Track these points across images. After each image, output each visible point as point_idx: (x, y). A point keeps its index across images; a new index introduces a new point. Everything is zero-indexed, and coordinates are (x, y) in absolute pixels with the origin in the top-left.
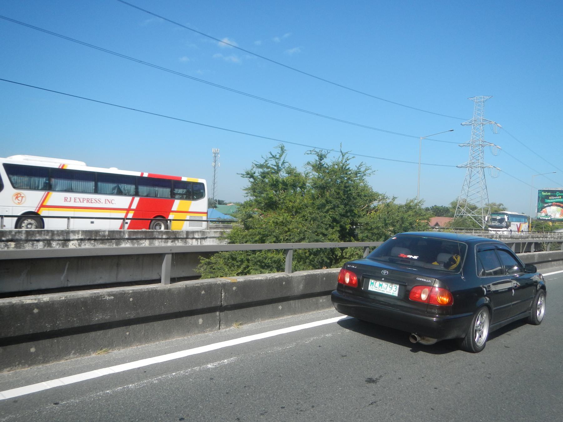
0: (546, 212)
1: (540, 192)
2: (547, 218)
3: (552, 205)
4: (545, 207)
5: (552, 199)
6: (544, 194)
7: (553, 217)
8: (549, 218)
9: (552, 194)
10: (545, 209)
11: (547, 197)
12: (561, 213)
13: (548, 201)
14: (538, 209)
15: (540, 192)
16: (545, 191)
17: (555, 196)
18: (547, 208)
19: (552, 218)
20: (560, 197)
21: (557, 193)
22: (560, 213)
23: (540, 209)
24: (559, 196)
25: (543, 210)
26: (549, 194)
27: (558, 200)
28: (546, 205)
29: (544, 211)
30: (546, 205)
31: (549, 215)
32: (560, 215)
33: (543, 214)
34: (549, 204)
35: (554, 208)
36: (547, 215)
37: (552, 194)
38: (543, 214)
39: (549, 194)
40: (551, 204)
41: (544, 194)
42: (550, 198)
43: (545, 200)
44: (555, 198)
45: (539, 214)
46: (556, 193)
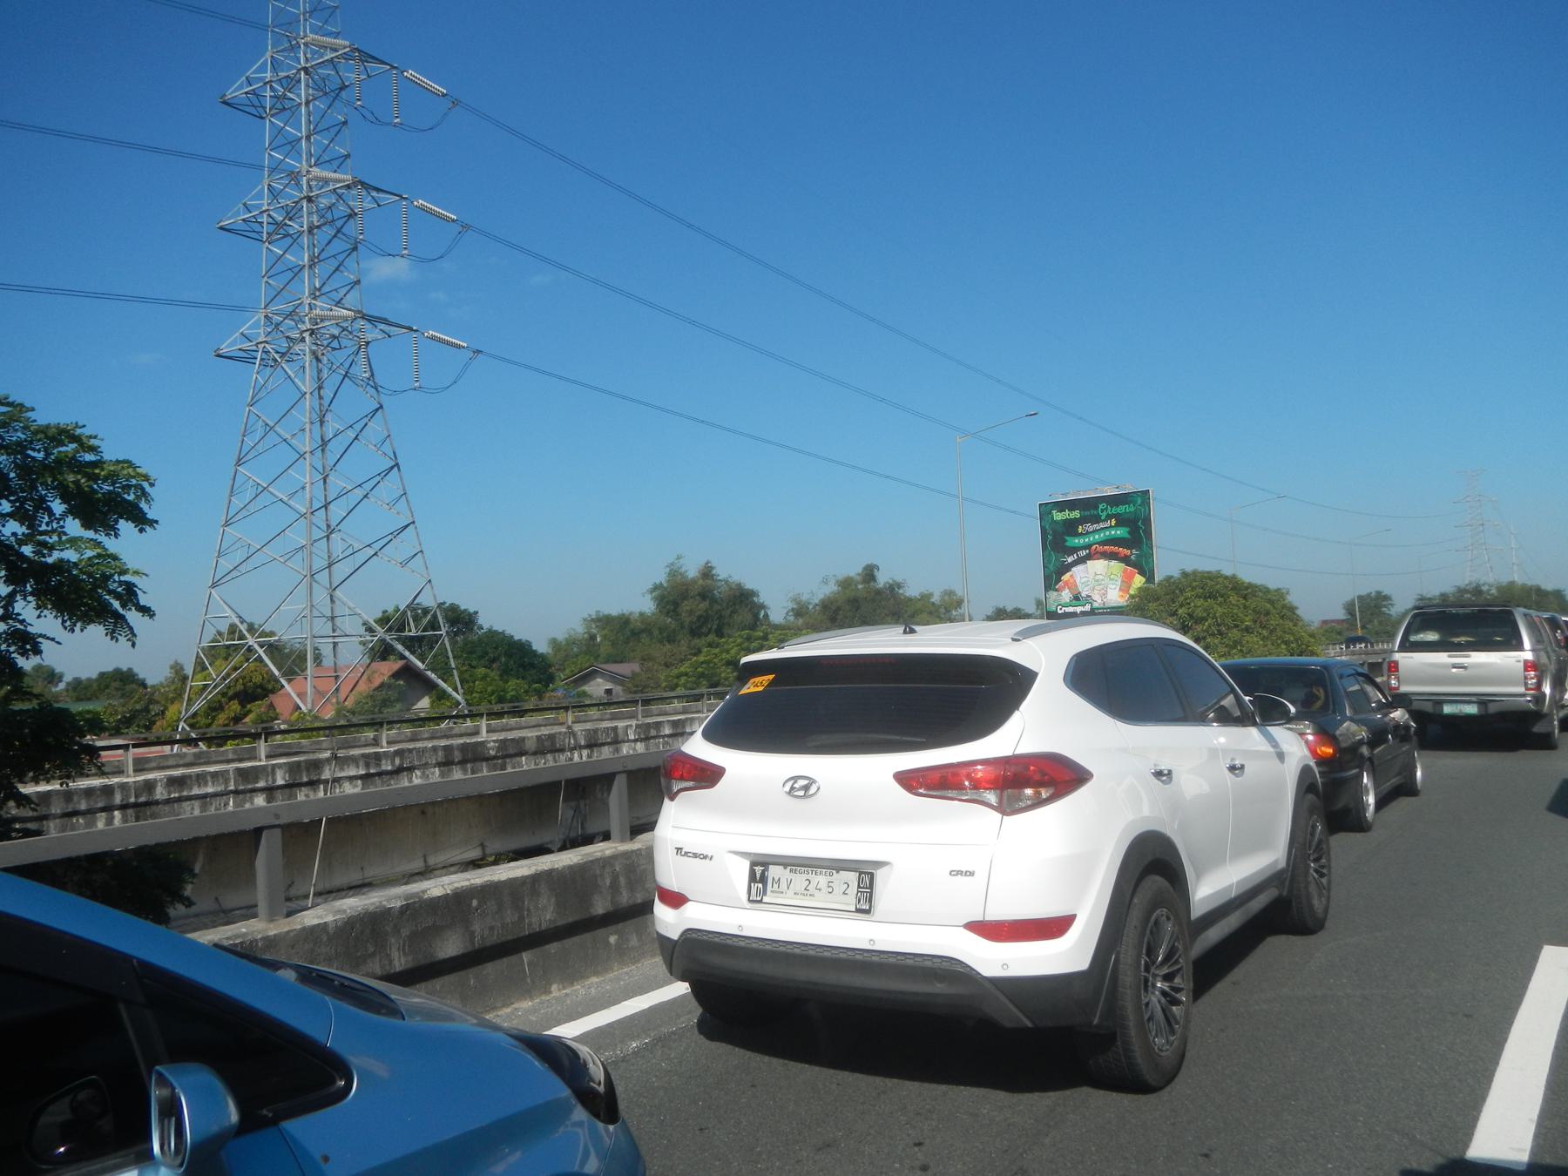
0: (1072, 586)
1: (1046, 510)
2: (1079, 609)
3: (1089, 557)
4: (1068, 568)
5: (1088, 533)
6: (1059, 516)
7: (1099, 601)
8: (1087, 608)
9: (1087, 513)
10: (1068, 575)
11: (1071, 527)
12: (1122, 581)
13: (1077, 541)
14: (1047, 578)
15: (1046, 510)
16: (1062, 506)
17: (1097, 520)
18: (1078, 571)
19: (1096, 605)
20: (1113, 522)
21: (1101, 507)
22: (1119, 583)
23: (1053, 578)
24: (1109, 517)
25: (1066, 577)
26: (1076, 514)
27: (1107, 533)
28: (1070, 560)
29: (1066, 583)
30: (1070, 560)
31: (1083, 595)
32: (1120, 589)
33: (1066, 595)
34: (1083, 553)
35: (1098, 566)
36: (1077, 598)
37: (1087, 513)
38: (1066, 595)
39: (1076, 514)
40: (1083, 553)
41: (1059, 516)
42: (1080, 530)
43: (1067, 538)
45: (1053, 595)
46: (1096, 507)
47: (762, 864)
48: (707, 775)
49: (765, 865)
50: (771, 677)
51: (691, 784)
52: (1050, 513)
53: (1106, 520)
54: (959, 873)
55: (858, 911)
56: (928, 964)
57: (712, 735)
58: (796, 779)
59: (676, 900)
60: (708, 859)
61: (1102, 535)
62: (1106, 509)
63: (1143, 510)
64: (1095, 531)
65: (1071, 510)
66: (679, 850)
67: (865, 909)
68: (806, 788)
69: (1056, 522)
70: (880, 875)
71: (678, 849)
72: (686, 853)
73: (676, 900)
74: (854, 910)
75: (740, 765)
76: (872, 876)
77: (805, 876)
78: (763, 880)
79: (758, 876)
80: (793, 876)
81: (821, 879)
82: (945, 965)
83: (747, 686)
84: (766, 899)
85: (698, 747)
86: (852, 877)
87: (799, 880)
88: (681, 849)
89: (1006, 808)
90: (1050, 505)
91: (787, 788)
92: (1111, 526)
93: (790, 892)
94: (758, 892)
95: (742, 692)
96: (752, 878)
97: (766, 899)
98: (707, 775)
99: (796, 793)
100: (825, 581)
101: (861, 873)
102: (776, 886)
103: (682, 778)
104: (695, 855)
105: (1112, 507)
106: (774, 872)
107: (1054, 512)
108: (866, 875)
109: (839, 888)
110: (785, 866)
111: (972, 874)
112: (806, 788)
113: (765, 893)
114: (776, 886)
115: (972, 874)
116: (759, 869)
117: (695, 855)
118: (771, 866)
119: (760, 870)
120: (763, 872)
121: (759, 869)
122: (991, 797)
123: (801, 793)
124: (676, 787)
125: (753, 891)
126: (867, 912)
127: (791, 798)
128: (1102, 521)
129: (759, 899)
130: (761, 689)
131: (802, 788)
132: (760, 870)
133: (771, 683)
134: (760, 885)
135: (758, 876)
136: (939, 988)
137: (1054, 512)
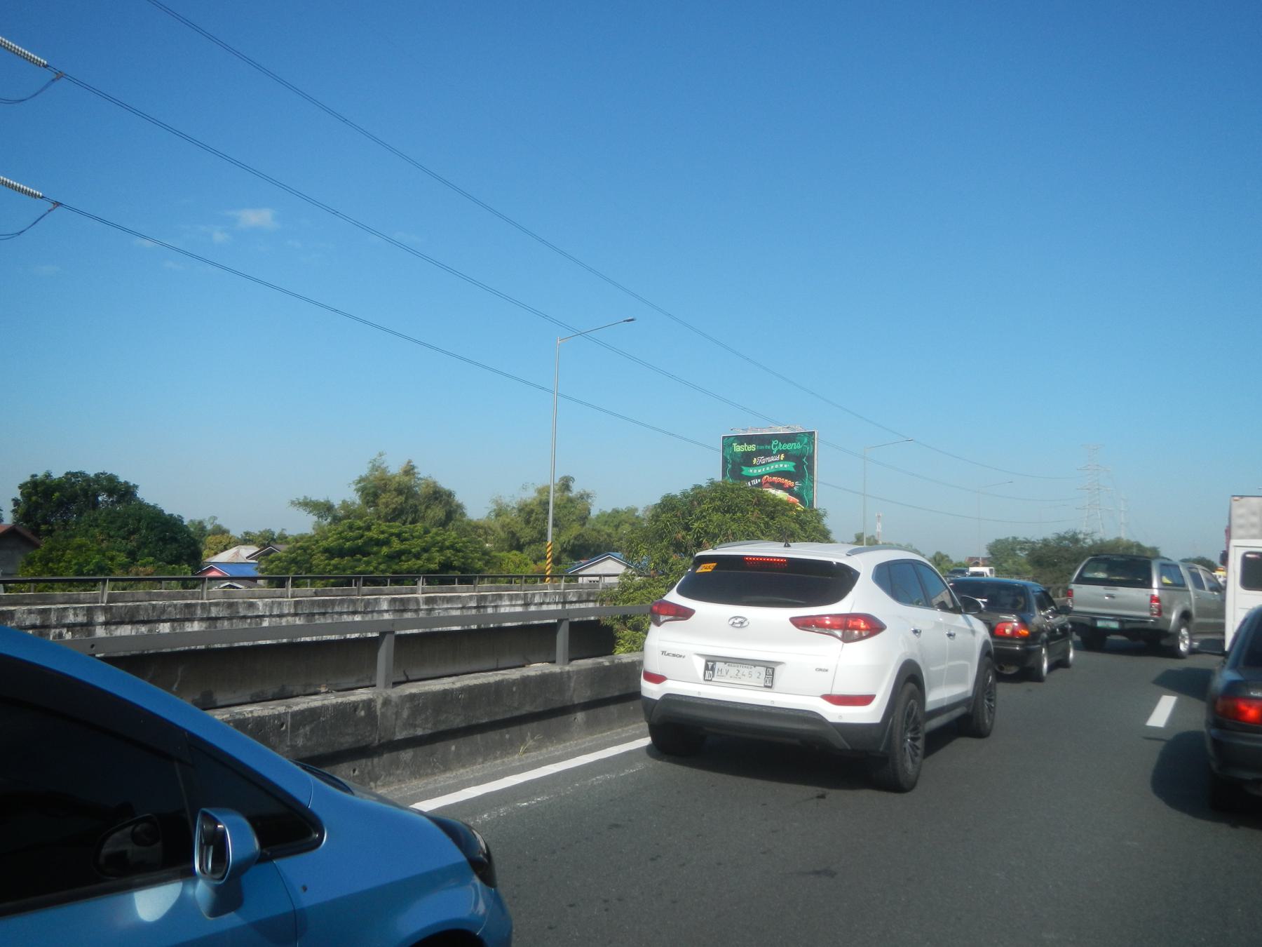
47: (712, 661)
48: (685, 614)
49: (714, 662)
50: (715, 564)
51: (671, 617)
54: (821, 670)
55: (766, 687)
56: (800, 714)
57: (684, 591)
58: (736, 618)
59: (658, 679)
60: (681, 658)
66: (663, 653)
67: (769, 686)
68: (742, 623)
70: (778, 669)
71: (663, 652)
72: (668, 654)
73: (658, 679)
74: (763, 685)
75: (704, 610)
76: (774, 669)
77: (736, 668)
78: (713, 669)
79: (710, 667)
80: (730, 668)
81: (745, 670)
82: (810, 715)
83: (701, 567)
84: (713, 679)
85: (674, 597)
86: (763, 670)
87: (733, 670)
88: (665, 652)
89: (846, 639)
91: (731, 622)
93: (728, 676)
94: (710, 676)
95: (697, 571)
96: (707, 668)
97: (713, 679)
98: (683, 614)
99: (736, 625)
101: (767, 668)
102: (720, 673)
103: (667, 615)
104: (674, 655)
106: (719, 665)
108: (770, 668)
109: (755, 675)
110: (726, 663)
111: (827, 671)
112: (742, 623)
113: (713, 676)
114: (720, 673)
115: (827, 671)
116: (710, 664)
117: (674, 655)
118: (717, 663)
119: (711, 664)
120: (713, 665)
121: (710, 664)
122: (839, 633)
123: (739, 625)
124: (662, 618)
125: (707, 675)
126: (770, 687)
127: (734, 629)
129: (710, 679)
130: (710, 570)
131: (741, 623)
132: (711, 664)
133: (715, 568)
134: (711, 672)
135: (710, 667)
136: (805, 727)
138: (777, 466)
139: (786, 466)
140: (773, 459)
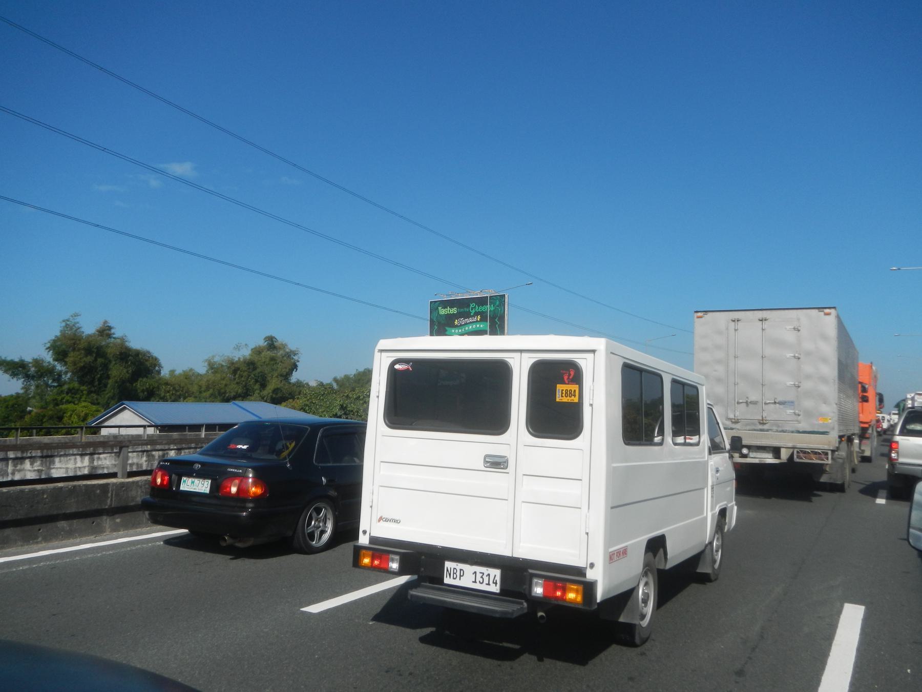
1: (434, 306)
5: (461, 325)
6: (443, 312)
9: (462, 310)
20: (479, 317)
21: (471, 306)
24: (476, 314)
26: (454, 311)
27: (474, 326)
37: (462, 310)
39: (454, 311)
41: (443, 312)
42: (456, 322)
43: (447, 328)
44: (467, 320)
46: (469, 306)
52: (437, 309)
53: (474, 316)
61: (470, 327)
62: (475, 307)
63: (499, 310)
64: (466, 324)
65: (451, 307)
69: (441, 316)
90: (439, 302)
92: (477, 321)
100: (238, 348)
105: (479, 306)
107: (440, 308)
128: (471, 317)
137: (440, 308)
138: (467, 328)
139: (482, 326)
140: (471, 320)
